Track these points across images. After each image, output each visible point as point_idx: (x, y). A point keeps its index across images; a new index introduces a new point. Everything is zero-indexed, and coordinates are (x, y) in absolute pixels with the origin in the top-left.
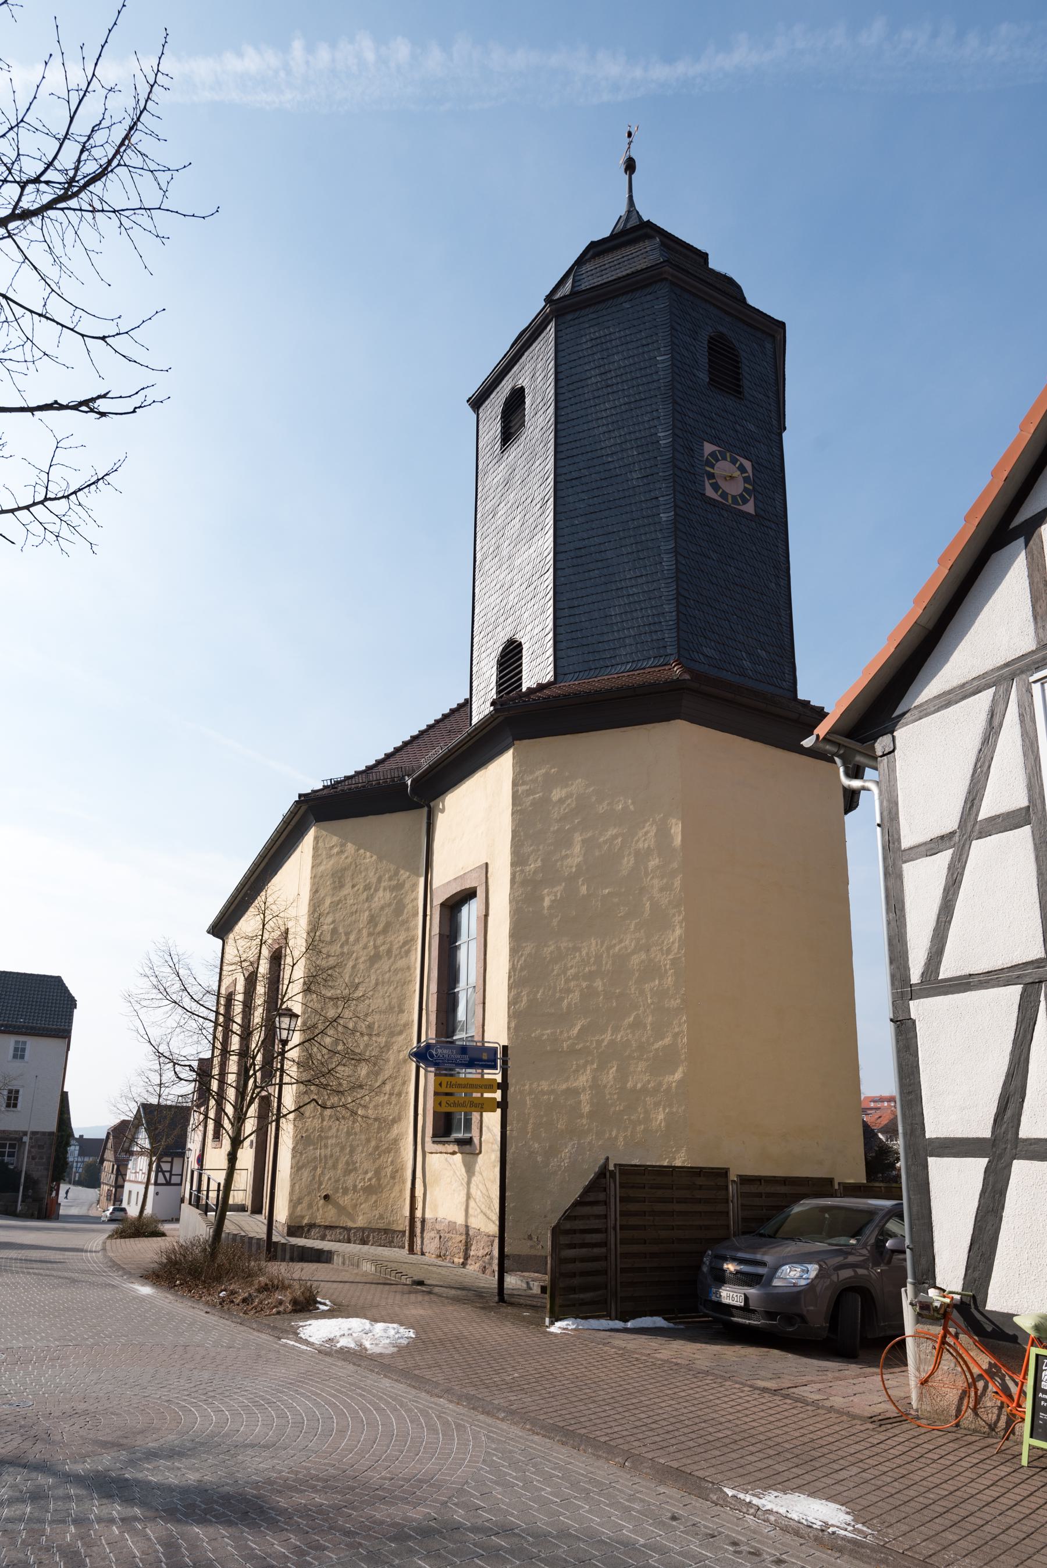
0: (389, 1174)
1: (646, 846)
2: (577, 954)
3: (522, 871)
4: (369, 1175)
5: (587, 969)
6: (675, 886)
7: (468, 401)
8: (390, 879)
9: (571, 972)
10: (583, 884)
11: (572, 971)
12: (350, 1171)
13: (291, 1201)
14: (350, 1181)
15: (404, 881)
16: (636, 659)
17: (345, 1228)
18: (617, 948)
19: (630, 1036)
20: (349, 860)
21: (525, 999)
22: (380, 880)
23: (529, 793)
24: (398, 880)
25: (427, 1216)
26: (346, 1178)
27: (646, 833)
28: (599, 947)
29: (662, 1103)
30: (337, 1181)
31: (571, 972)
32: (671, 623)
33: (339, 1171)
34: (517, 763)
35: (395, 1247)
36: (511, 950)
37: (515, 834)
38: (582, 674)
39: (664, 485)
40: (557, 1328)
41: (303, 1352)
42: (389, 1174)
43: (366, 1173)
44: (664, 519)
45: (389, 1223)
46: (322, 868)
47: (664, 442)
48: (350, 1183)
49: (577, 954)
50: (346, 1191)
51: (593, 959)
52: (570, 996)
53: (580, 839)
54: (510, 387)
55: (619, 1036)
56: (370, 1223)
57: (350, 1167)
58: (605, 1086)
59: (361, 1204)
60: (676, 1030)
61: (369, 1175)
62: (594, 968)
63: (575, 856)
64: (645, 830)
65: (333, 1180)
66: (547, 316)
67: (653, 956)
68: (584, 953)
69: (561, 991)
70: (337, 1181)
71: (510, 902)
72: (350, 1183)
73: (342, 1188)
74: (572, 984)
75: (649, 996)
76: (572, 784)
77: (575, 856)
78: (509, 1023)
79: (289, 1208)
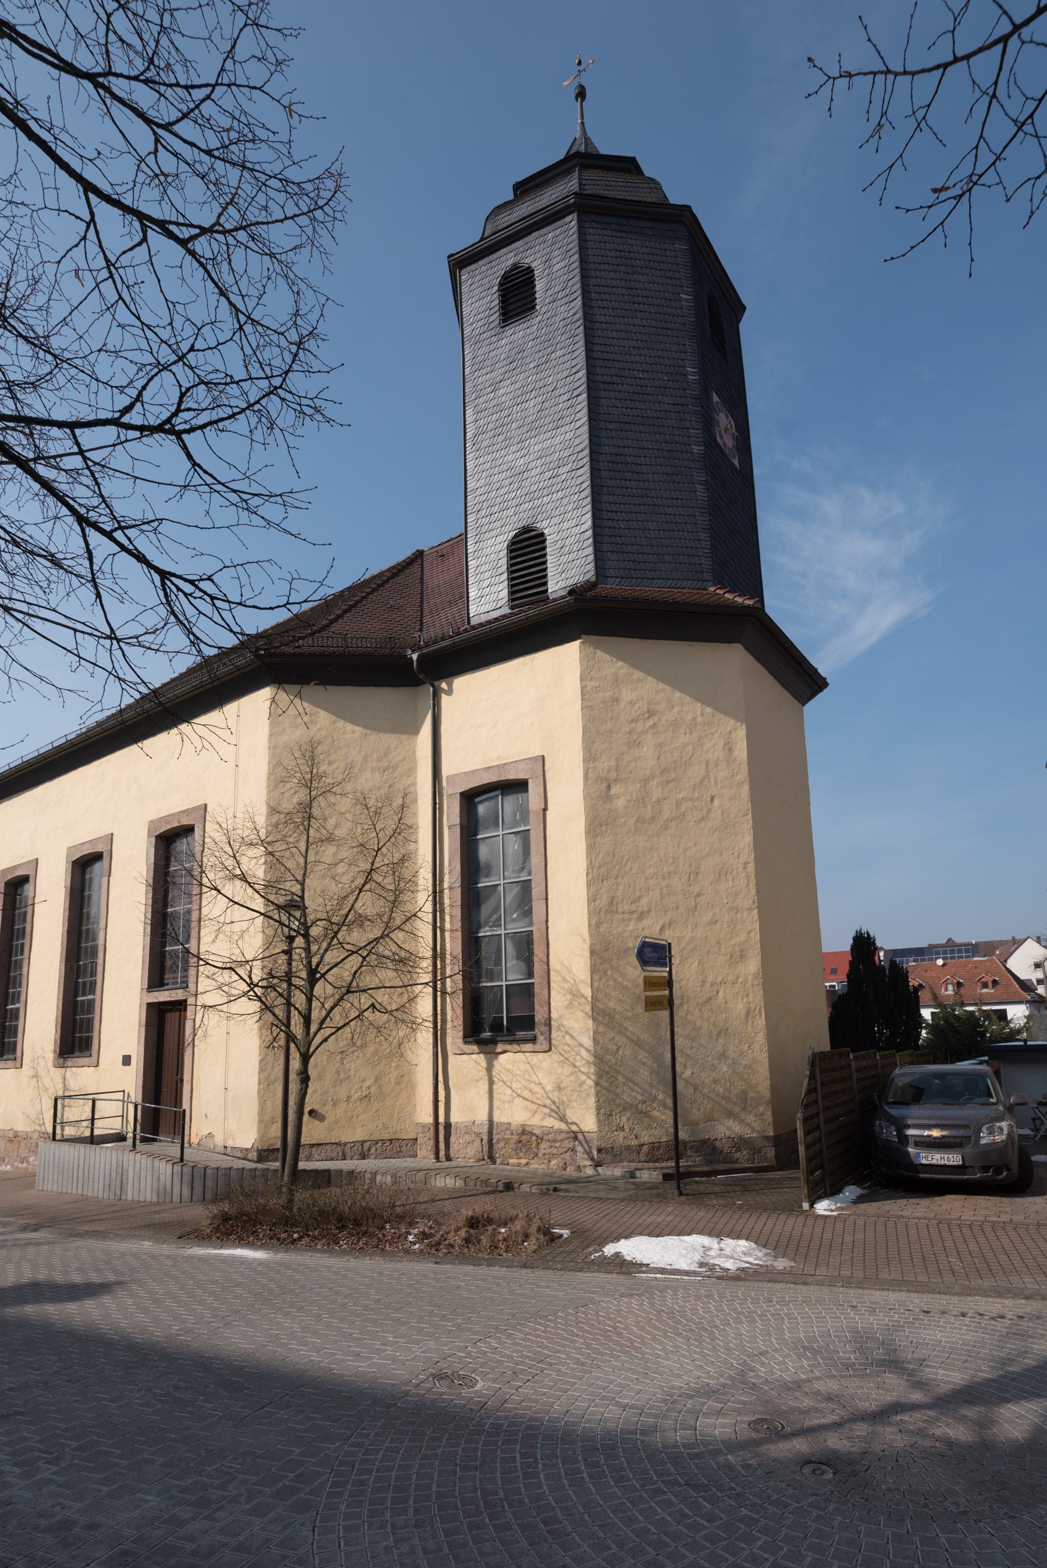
0: (393, 1080)
1: (715, 757)
2: (656, 854)
3: (595, 768)
4: (368, 1083)
5: (665, 869)
6: (743, 796)
7: (449, 257)
8: (379, 760)
9: (649, 872)
10: (657, 787)
11: (652, 870)
12: (342, 1081)
13: (260, 1121)
14: (342, 1092)
15: (398, 764)
16: (676, 577)
17: (339, 1144)
18: (693, 851)
19: (709, 933)
20: (323, 733)
21: (605, 896)
22: (365, 759)
23: (597, 690)
24: (390, 762)
25: (453, 1119)
26: (338, 1088)
27: (714, 745)
28: (676, 848)
29: (741, 993)
30: (326, 1092)
31: (650, 872)
32: (706, 551)
33: (327, 1082)
34: (584, 658)
35: (404, 1157)
36: (587, 846)
37: (586, 730)
38: (624, 580)
39: (694, 419)
40: (823, 1207)
41: (695, 1282)
42: (393, 1080)
43: (363, 1081)
44: (696, 451)
45: (396, 1132)
46: (283, 739)
47: (693, 377)
48: (342, 1093)
49: (656, 854)
50: (335, 1103)
51: (671, 860)
52: (651, 895)
53: (653, 742)
54: (511, 261)
55: (699, 933)
56: (371, 1135)
57: (342, 1076)
58: (688, 980)
59: (358, 1116)
60: (750, 928)
61: (368, 1083)
62: (672, 869)
63: (647, 756)
64: (713, 742)
65: (319, 1093)
66: (569, 206)
67: (726, 859)
68: (662, 853)
69: (641, 889)
70: (326, 1092)
71: (584, 798)
72: (342, 1093)
73: (332, 1100)
74: (652, 882)
75: (724, 896)
76: (642, 688)
77: (647, 756)
78: (589, 920)
79: (259, 1130)
